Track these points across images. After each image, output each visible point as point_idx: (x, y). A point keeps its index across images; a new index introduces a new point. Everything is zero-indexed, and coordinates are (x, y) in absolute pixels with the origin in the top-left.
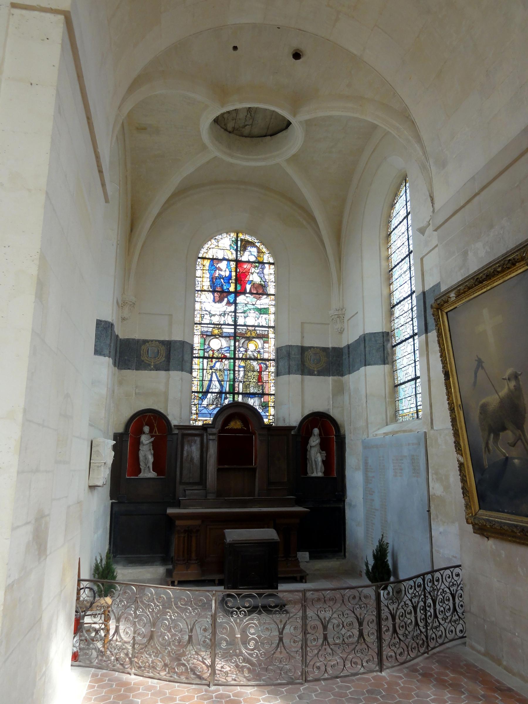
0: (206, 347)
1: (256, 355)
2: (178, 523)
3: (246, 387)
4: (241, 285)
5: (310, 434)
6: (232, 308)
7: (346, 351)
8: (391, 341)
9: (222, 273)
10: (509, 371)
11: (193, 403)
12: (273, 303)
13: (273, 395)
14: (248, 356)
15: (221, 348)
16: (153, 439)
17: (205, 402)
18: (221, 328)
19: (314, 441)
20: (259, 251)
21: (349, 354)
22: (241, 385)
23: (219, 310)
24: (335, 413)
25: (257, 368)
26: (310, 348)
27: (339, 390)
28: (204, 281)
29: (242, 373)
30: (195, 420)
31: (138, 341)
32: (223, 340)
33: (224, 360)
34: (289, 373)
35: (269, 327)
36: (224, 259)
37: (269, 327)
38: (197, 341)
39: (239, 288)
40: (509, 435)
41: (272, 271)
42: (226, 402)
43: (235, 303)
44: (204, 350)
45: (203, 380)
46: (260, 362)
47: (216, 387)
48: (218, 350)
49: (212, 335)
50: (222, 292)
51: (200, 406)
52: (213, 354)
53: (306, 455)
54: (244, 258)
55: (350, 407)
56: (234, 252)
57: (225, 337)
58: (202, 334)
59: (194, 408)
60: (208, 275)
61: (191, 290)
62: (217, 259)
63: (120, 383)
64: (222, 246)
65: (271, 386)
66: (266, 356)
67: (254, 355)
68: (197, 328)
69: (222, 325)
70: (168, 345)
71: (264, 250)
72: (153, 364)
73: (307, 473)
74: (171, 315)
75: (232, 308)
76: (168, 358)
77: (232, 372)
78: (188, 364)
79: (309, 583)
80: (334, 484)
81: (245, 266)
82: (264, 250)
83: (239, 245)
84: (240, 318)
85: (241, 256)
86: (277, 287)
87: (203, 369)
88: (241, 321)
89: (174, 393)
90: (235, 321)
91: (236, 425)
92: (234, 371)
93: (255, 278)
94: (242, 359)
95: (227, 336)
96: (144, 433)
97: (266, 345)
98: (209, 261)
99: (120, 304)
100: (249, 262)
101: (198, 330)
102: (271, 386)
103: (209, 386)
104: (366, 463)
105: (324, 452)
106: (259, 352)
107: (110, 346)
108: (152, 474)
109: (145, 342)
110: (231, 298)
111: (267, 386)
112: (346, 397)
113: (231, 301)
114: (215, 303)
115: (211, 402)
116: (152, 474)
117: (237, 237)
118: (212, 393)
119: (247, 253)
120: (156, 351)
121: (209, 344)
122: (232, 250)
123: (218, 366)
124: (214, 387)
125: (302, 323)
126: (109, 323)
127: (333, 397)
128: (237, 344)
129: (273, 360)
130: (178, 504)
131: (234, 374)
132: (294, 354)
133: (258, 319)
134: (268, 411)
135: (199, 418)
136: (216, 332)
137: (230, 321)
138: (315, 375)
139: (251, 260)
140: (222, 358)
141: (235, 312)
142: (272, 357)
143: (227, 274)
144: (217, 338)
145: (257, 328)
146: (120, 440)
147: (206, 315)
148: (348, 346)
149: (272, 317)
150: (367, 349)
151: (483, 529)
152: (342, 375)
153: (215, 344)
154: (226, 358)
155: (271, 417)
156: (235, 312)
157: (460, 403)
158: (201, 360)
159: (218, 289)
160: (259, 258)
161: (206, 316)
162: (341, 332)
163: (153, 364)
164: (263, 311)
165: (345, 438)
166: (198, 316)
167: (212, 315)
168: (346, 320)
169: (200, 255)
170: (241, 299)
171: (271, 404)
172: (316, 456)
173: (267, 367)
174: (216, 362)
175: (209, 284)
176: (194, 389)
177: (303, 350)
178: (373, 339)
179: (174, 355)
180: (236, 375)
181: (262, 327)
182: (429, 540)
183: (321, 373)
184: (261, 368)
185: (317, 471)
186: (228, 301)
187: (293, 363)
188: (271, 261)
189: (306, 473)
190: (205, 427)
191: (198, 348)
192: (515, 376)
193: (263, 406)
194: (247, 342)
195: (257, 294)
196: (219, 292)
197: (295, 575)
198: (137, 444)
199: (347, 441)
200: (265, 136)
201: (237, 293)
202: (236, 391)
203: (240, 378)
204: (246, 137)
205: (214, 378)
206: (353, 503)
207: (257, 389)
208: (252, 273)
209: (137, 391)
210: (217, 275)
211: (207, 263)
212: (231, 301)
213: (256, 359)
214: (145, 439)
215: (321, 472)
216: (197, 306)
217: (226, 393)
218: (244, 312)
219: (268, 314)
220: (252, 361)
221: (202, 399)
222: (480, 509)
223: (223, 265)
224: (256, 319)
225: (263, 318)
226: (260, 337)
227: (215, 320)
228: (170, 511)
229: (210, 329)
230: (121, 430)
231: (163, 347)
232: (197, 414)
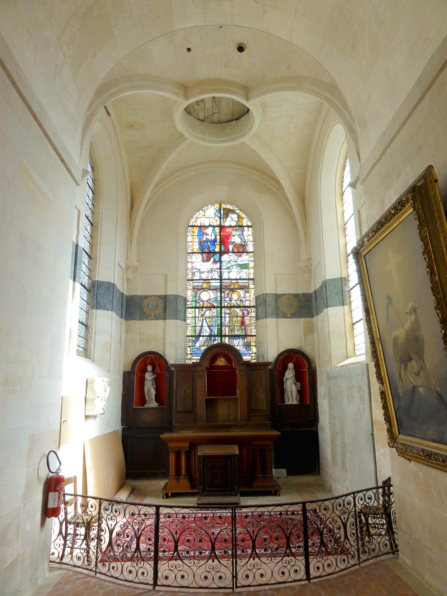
0: (197, 298)
1: (238, 303)
2: (170, 445)
3: (231, 330)
4: (225, 246)
5: (285, 368)
6: (218, 265)
7: (314, 296)
8: (348, 284)
9: (209, 237)
10: (410, 305)
11: (188, 345)
12: (252, 259)
13: (255, 336)
14: (232, 305)
15: (210, 299)
16: (155, 376)
17: (198, 344)
18: (209, 283)
19: (290, 374)
20: (239, 217)
21: (316, 298)
22: (227, 328)
23: (206, 268)
24: (307, 350)
26: (283, 295)
27: (310, 330)
29: (227, 319)
30: (190, 359)
31: (141, 297)
32: (211, 292)
33: (212, 309)
35: (249, 279)
36: (210, 226)
37: (249, 279)
38: (189, 294)
39: (223, 249)
40: (414, 365)
41: (250, 233)
42: (215, 343)
43: (220, 261)
44: (196, 301)
45: (195, 326)
46: (242, 309)
48: (207, 301)
49: (202, 289)
50: (209, 252)
51: (193, 347)
52: (203, 304)
53: (283, 386)
54: (227, 224)
55: (319, 344)
56: (218, 219)
57: (213, 289)
58: (194, 288)
59: (189, 349)
60: (197, 240)
62: (203, 226)
63: (127, 331)
65: (253, 328)
66: (247, 304)
67: (237, 304)
68: (190, 284)
69: (209, 280)
70: (165, 298)
71: (243, 215)
72: (152, 314)
73: (285, 402)
74: (166, 275)
75: (218, 265)
76: (165, 309)
77: (219, 318)
78: (182, 314)
79: (283, 495)
80: (308, 411)
81: (227, 230)
82: (243, 215)
83: (222, 213)
84: (225, 273)
85: (224, 222)
86: (254, 246)
87: (195, 317)
88: (225, 276)
90: (221, 276)
91: (221, 362)
92: (221, 317)
93: (236, 239)
94: (227, 307)
95: (215, 289)
96: (148, 371)
97: (247, 295)
98: (198, 228)
99: (124, 268)
100: (230, 226)
102: (253, 328)
103: (201, 331)
104: (330, 392)
105: (299, 383)
106: (241, 300)
107: (113, 302)
109: (146, 297)
110: (217, 257)
111: (249, 329)
112: (316, 336)
113: (217, 260)
114: (204, 262)
115: (203, 344)
116: (154, 404)
117: (220, 206)
118: (203, 336)
119: (229, 219)
120: (155, 304)
121: (199, 297)
122: (216, 218)
123: (208, 313)
124: (205, 331)
126: (111, 283)
127: (304, 336)
128: (223, 295)
129: (254, 307)
130: (171, 430)
131: (221, 320)
132: (270, 301)
133: (240, 273)
134: (250, 350)
135: (193, 358)
136: (205, 286)
137: (216, 276)
138: (288, 318)
139: (232, 225)
140: (210, 307)
141: (220, 268)
142: (253, 304)
143: (213, 238)
144: (206, 291)
145: (239, 281)
146: (127, 378)
147: (196, 273)
148: (315, 292)
149: (252, 271)
150: (328, 293)
151: (405, 452)
152: (312, 317)
153: (205, 296)
154: (213, 307)
155: (253, 355)
156: (220, 268)
157: (379, 337)
158: (194, 309)
159: (206, 250)
160: (239, 223)
161: (196, 274)
162: (309, 281)
163: (152, 314)
164: (244, 266)
165: (316, 371)
166: (190, 273)
167: (201, 273)
168: (313, 269)
169: (191, 224)
170: (225, 257)
173: (248, 313)
174: (206, 311)
175: (198, 247)
176: (189, 334)
178: (332, 284)
179: (168, 307)
180: (223, 320)
181: (244, 279)
182: (373, 461)
184: (243, 314)
186: (214, 260)
188: (250, 224)
189: (284, 401)
190: (195, 365)
191: (190, 300)
192: (414, 310)
193: (246, 346)
194: (231, 292)
195: (238, 252)
196: (207, 253)
197: (270, 489)
198: (142, 381)
199: (318, 373)
200: (232, 120)
201: (221, 253)
202: (223, 334)
203: (226, 323)
204: (216, 123)
205: (205, 324)
206: (324, 427)
207: (240, 331)
208: (234, 236)
209: (141, 337)
210: (204, 239)
211: (196, 230)
212: (217, 260)
213: (239, 307)
214: (149, 376)
215: (296, 400)
216: (189, 265)
217: (215, 336)
218: (228, 268)
219: (249, 269)
220: (235, 309)
221: (195, 342)
222: (399, 434)
223: (209, 231)
224: (238, 273)
225: (244, 272)
226: (241, 288)
227: (204, 276)
228: (165, 436)
229: (200, 284)
230: (129, 369)
231: (161, 301)
232: (191, 354)
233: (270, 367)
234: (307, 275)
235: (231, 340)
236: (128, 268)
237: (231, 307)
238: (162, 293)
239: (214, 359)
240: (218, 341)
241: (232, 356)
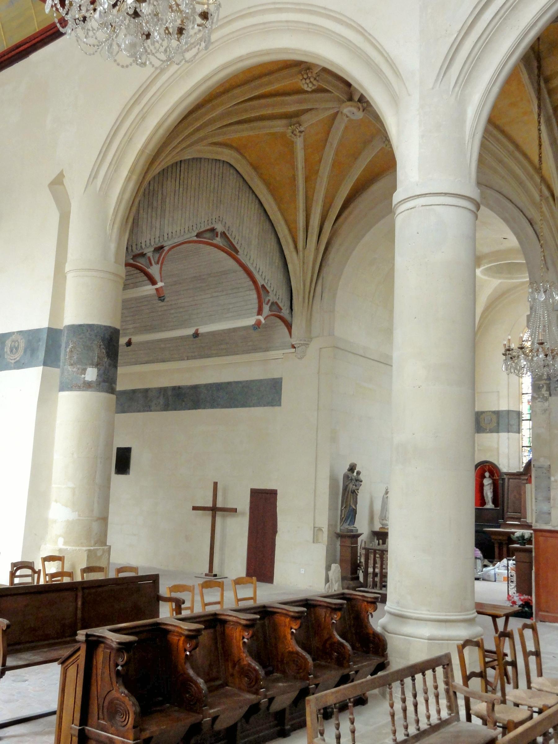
70: (497, 413)
74: (498, 392)
76: (498, 423)
78: (515, 427)
89: (503, 449)
214: (487, 482)
238: (497, 410)
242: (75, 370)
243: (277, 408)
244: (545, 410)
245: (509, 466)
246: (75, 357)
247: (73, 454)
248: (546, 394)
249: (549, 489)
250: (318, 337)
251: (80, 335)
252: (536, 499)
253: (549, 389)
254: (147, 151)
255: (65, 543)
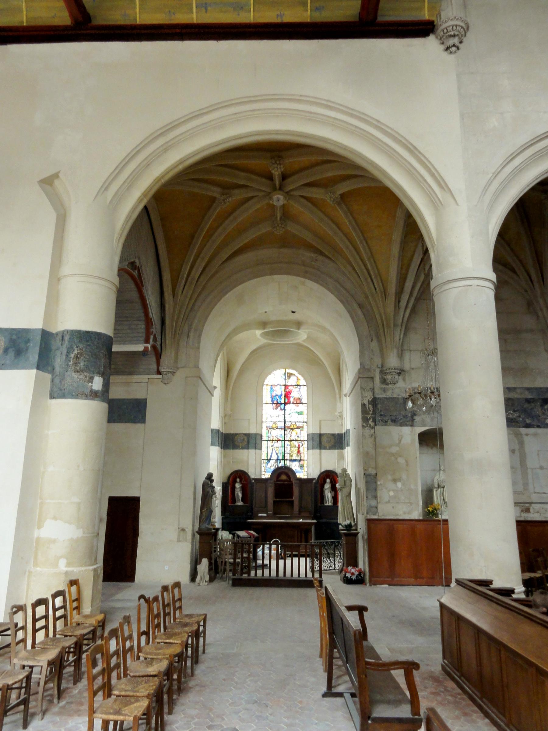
0: (269, 434)
5: (325, 482)
19: (327, 486)
20: (298, 379)
25: (297, 445)
28: (266, 397)
31: (233, 434)
34: (313, 449)
39: (286, 401)
47: (274, 457)
50: (278, 403)
58: (267, 428)
61: (259, 403)
63: (225, 456)
64: (276, 378)
70: (248, 435)
74: (249, 420)
76: (248, 442)
89: (252, 461)
90: (285, 420)
91: (284, 477)
92: (284, 447)
93: (295, 394)
101: (264, 425)
103: (271, 456)
108: (240, 503)
109: (236, 434)
125: (320, 421)
136: (274, 426)
141: (285, 414)
154: (280, 440)
156: (285, 414)
159: (275, 402)
162: (342, 425)
164: (300, 413)
170: (287, 406)
171: (305, 465)
172: (328, 495)
177: (321, 435)
179: (252, 441)
183: (330, 448)
184: (299, 445)
185: (329, 502)
187: (315, 443)
189: (323, 504)
190: (266, 480)
198: (234, 488)
201: (285, 404)
213: (296, 441)
214: (238, 485)
217: (280, 460)
221: (267, 463)
226: (298, 428)
230: (226, 481)
233: (314, 481)
234: (340, 421)
235: (291, 463)
236: (225, 416)
237: (291, 441)
239: (279, 475)
240: (281, 464)
241: (290, 475)
242: (81, 377)
243: (140, 426)
244: (372, 435)
245: (255, 474)
246: (82, 364)
247: (78, 466)
248: (372, 424)
249: (376, 490)
250: (183, 367)
251: (87, 341)
252: (367, 497)
253: (374, 421)
254: (163, 181)
255: (68, 565)
